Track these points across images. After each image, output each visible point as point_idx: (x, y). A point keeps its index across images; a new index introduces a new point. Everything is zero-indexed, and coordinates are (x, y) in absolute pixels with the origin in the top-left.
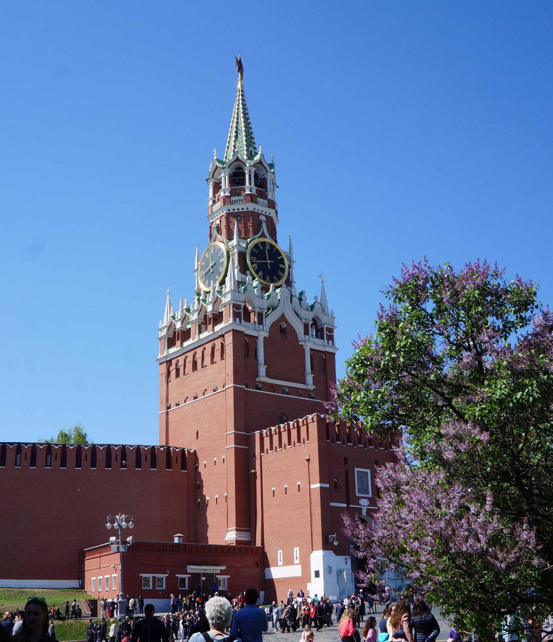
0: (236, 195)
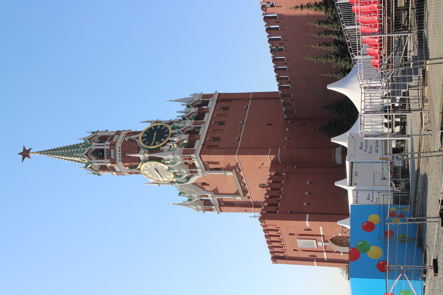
0: (111, 155)
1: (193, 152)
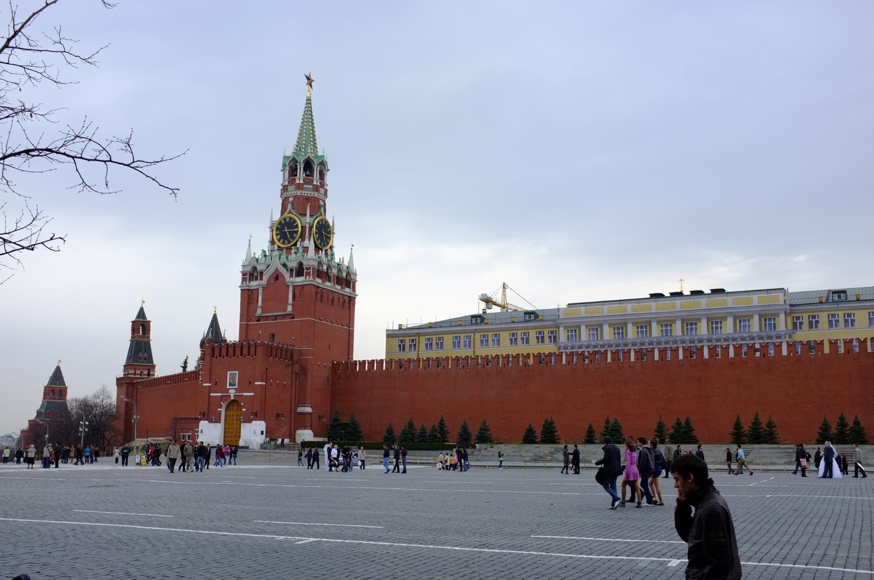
1: (314, 278)
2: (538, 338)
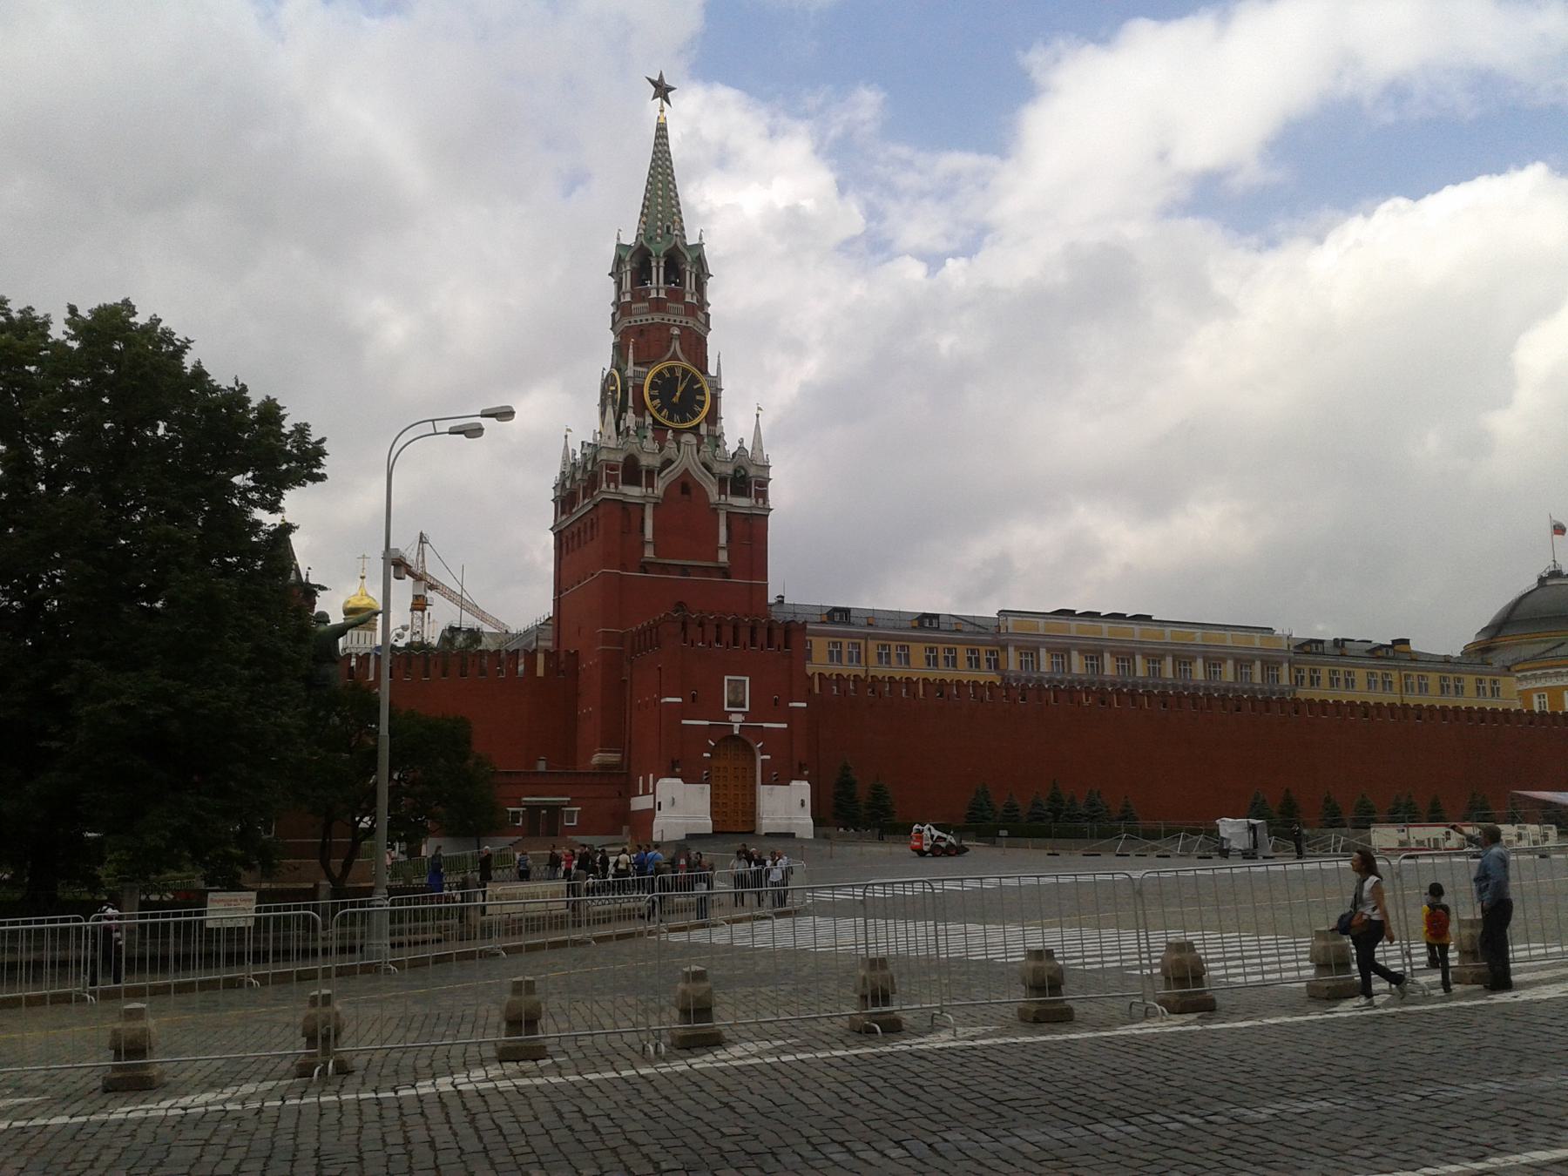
2: (969, 659)
